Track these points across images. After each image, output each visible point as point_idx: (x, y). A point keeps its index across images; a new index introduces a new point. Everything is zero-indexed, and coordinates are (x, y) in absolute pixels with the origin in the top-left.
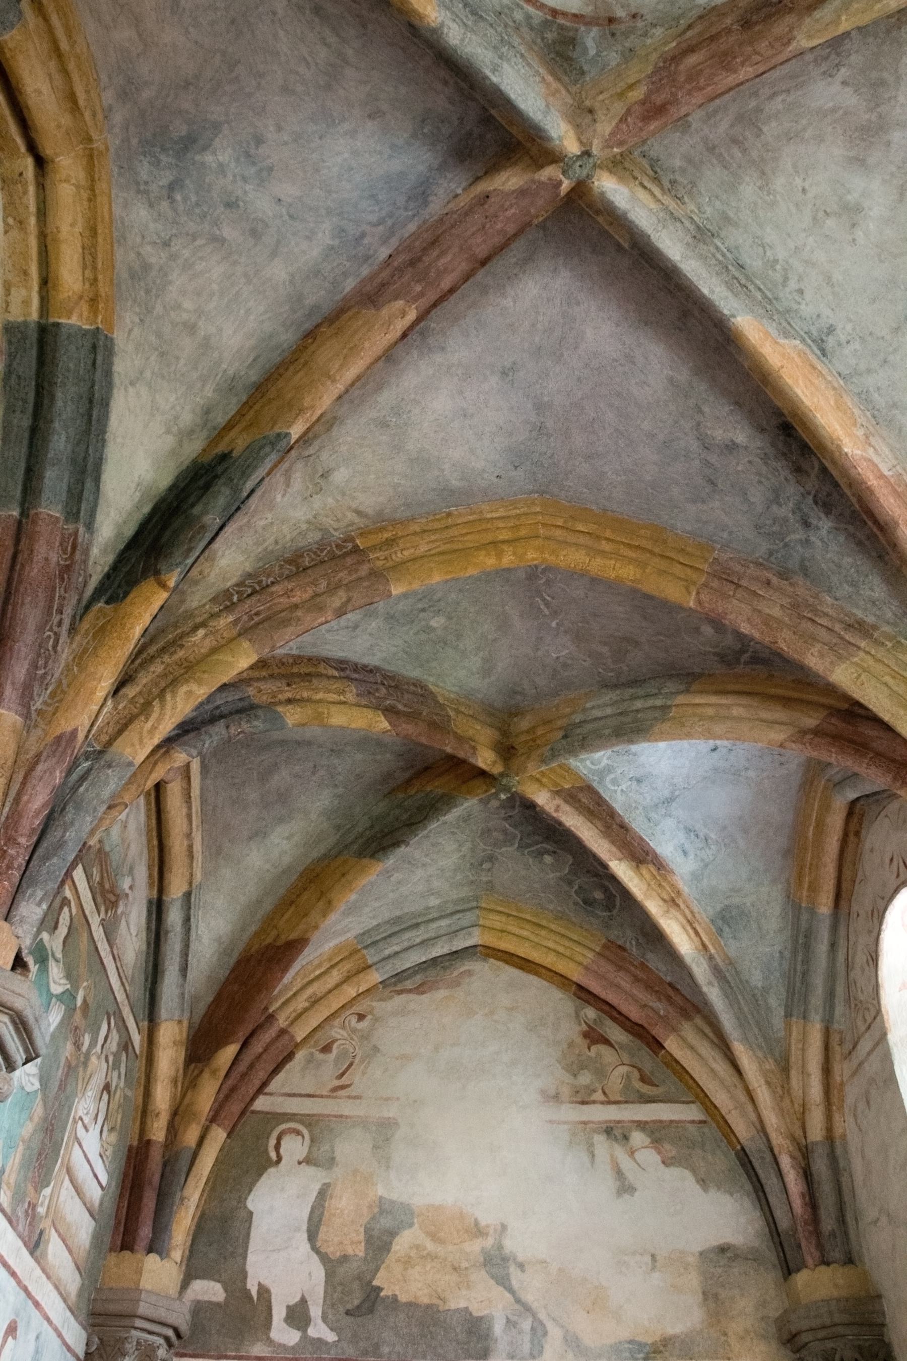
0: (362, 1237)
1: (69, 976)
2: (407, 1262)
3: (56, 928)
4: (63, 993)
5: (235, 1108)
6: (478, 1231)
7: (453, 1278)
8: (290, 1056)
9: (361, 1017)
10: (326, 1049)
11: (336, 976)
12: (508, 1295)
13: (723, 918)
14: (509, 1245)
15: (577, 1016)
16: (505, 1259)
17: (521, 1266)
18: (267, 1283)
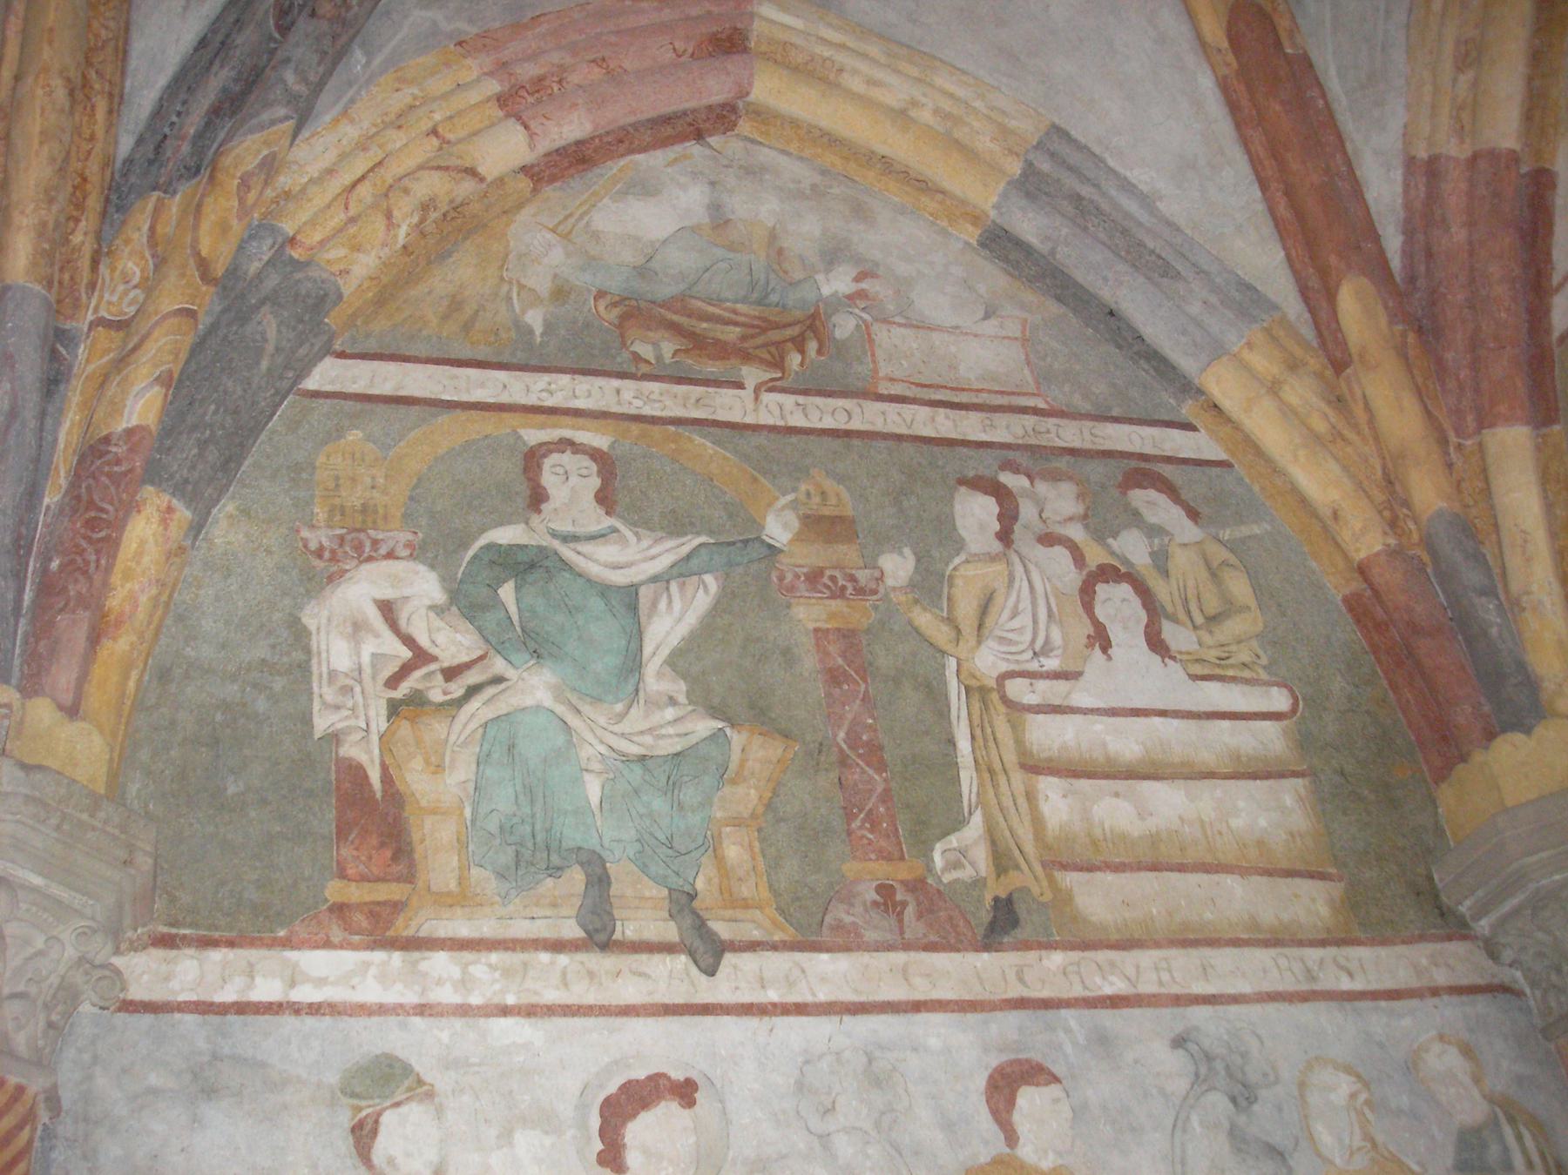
1: (676, 525)
3: (537, 498)
4: (689, 557)
8: (1541, 183)
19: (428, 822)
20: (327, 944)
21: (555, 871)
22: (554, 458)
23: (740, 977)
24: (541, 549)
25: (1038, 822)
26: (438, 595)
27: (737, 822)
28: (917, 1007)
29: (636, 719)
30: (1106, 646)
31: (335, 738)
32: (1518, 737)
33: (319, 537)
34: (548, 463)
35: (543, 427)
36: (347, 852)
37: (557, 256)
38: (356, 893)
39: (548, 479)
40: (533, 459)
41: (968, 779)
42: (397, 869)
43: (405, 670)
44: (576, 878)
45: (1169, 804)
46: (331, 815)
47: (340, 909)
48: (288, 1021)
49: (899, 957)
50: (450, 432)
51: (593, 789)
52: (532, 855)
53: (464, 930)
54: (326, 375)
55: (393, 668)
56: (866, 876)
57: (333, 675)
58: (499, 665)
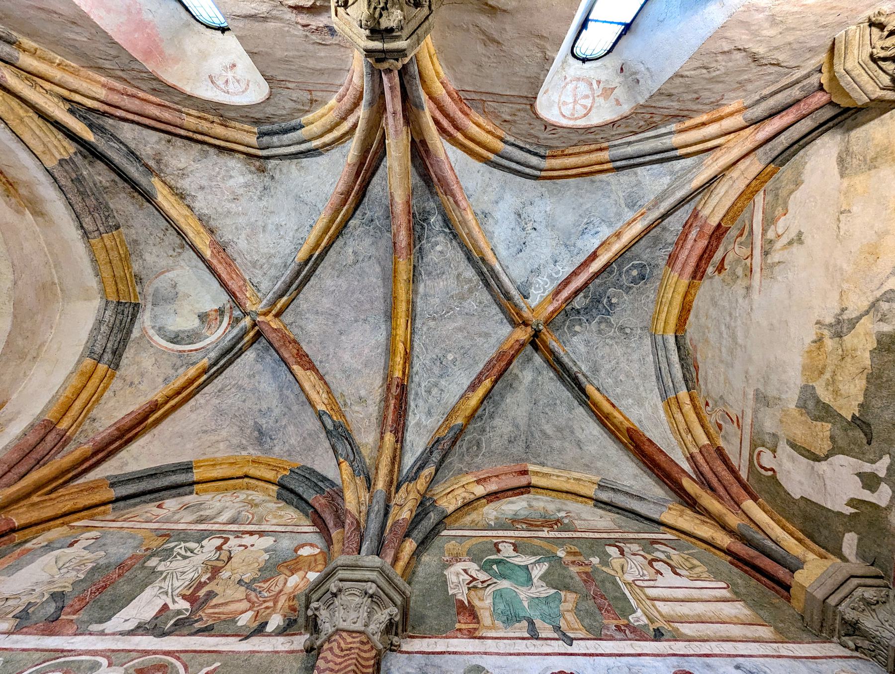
0: (819, 424)
1: (534, 554)
2: (836, 393)
5: (736, 489)
6: (819, 340)
7: (849, 359)
8: (720, 451)
9: (707, 404)
10: (720, 427)
11: (679, 416)
12: (862, 321)
13: (634, 206)
14: (829, 319)
15: (711, 278)
16: (839, 322)
17: (843, 310)
18: (846, 499)
20: (457, 637)
21: (519, 621)
23: (579, 647)
25: (658, 611)
27: (568, 611)
28: (640, 655)
29: (533, 590)
30: (661, 574)
32: (800, 571)
36: (460, 617)
37: (495, 513)
38: (463, 626)
39: (500, 547)
40: (496, 545)
41: (632, 601)
43: (471, 582)
44: (525, 623)
45: (699, 608)
47: (460, 630)
48: (447, 656)
49: (629, 642)
50: (474, 541)
51: (526, 604)
52: (511, 618)
53: (495, 635)
54: (444, 533)
56: (612, 623)
58: (495, 580)
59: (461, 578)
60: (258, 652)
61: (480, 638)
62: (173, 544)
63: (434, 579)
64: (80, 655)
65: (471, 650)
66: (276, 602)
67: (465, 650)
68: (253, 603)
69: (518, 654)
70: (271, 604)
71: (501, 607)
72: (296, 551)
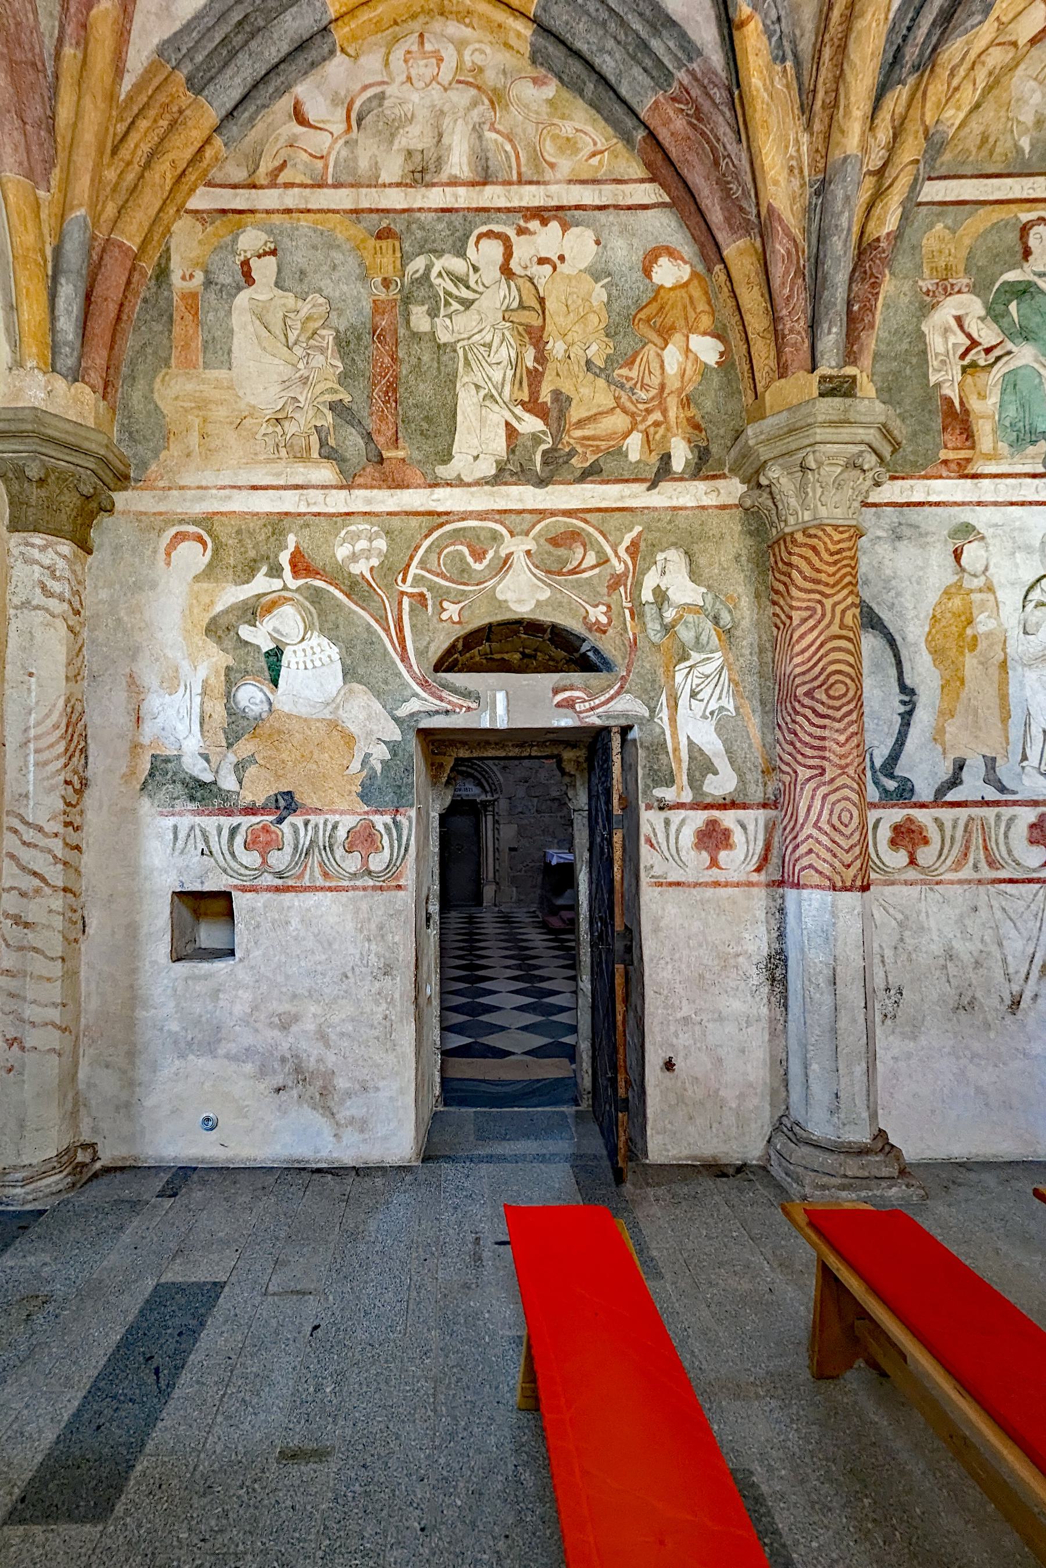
3: (1027, 253)
19: (981, 422)
20: (941, 477)
22: (1036, 229)
24: (1029, 282)
26: (982, 313)
31: (938, 385)
33: (926, 284)
34: (1032, 232)
35: (1029, 211)
36: (947, 437)
38: (951, 455)
39: (1032, 242)
42: (968, 444)
46: (940, 420)
47: (945, 462)
48: (927, 508)
55: (962, 350)
57: (937, 355)
58: (1009, 346)
59: (952, 340)
60: (681, 509)
61: (975, 476)
62: (419, 264)
63: (905, 346)
64: (463, 519)
65: (959, 498)
66: (665, 413)
67: (952, 499)
68: (633, 415)
69: (1023, 504)
70: (657, 416)
71: (1012, 411)
72: (647, 273)
